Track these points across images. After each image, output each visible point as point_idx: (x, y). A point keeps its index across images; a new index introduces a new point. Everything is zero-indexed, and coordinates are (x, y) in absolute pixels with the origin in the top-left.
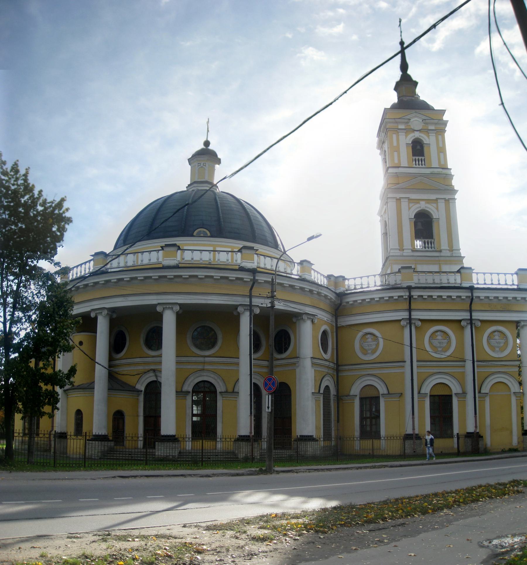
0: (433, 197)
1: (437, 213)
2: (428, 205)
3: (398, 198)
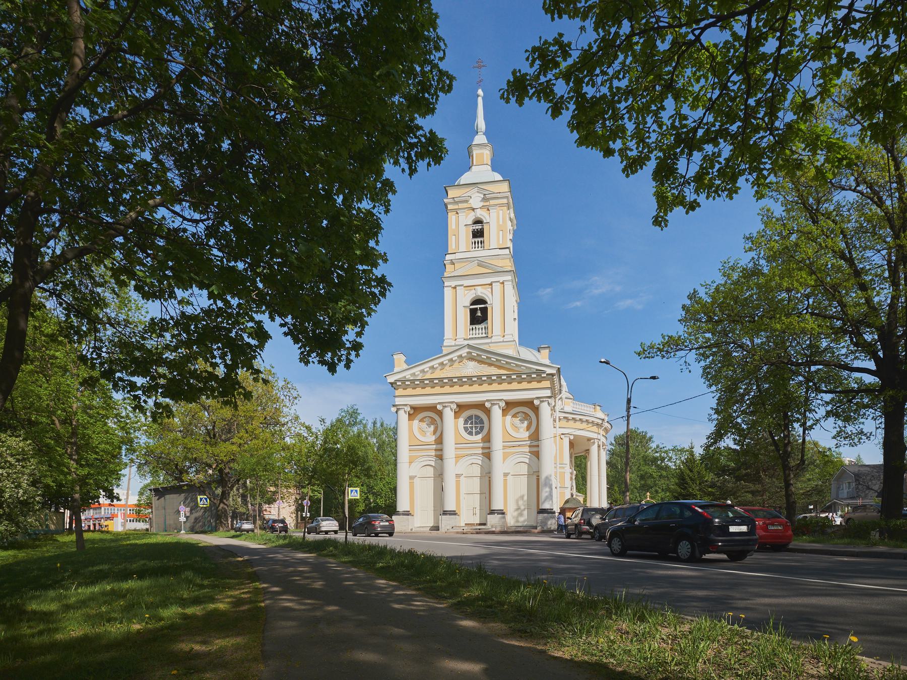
2: (484, 291)
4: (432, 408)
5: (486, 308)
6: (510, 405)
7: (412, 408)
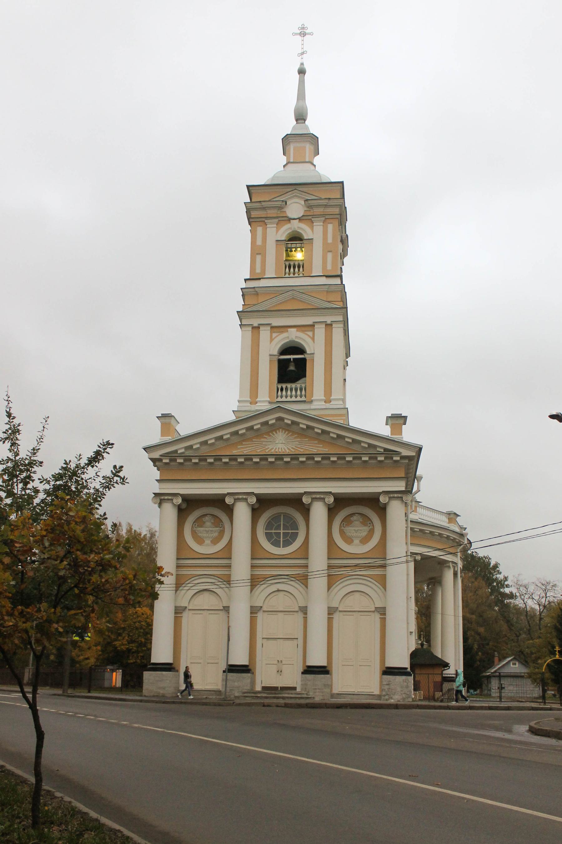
0: (308, 320)
3: (256, 325)
5: (304, 361)
6: (340, 502)
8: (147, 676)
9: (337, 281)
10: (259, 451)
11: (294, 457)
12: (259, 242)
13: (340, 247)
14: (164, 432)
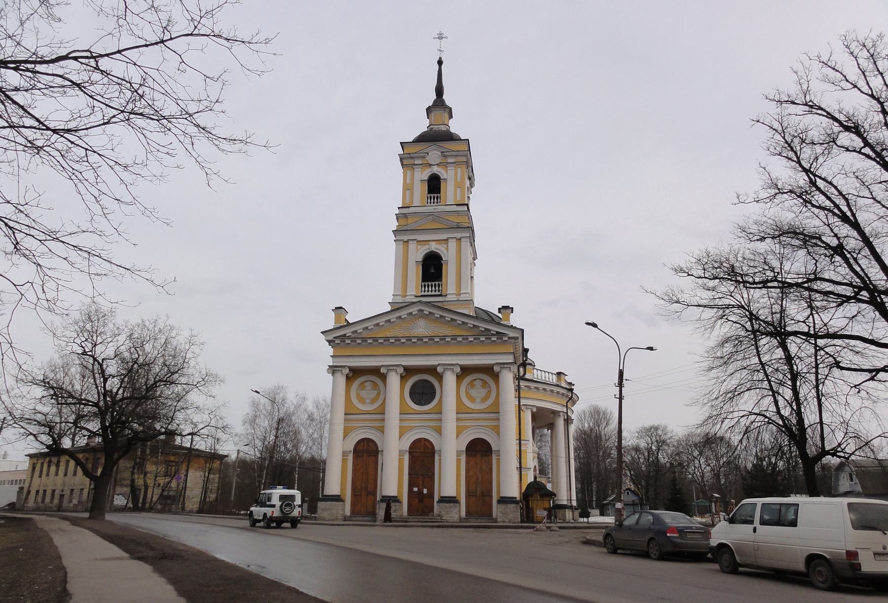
0: (444, 236)
1: (448, 254)
2: (439, 247)
4: (375, 371)
6: (465, 371)
7: (352, 369)
8: (320, 505)
9: (465, 208)
10: (406, 334)
11: (431, 338)
12: (408, 181)
13: (468, 182)
14: (337, 320)
